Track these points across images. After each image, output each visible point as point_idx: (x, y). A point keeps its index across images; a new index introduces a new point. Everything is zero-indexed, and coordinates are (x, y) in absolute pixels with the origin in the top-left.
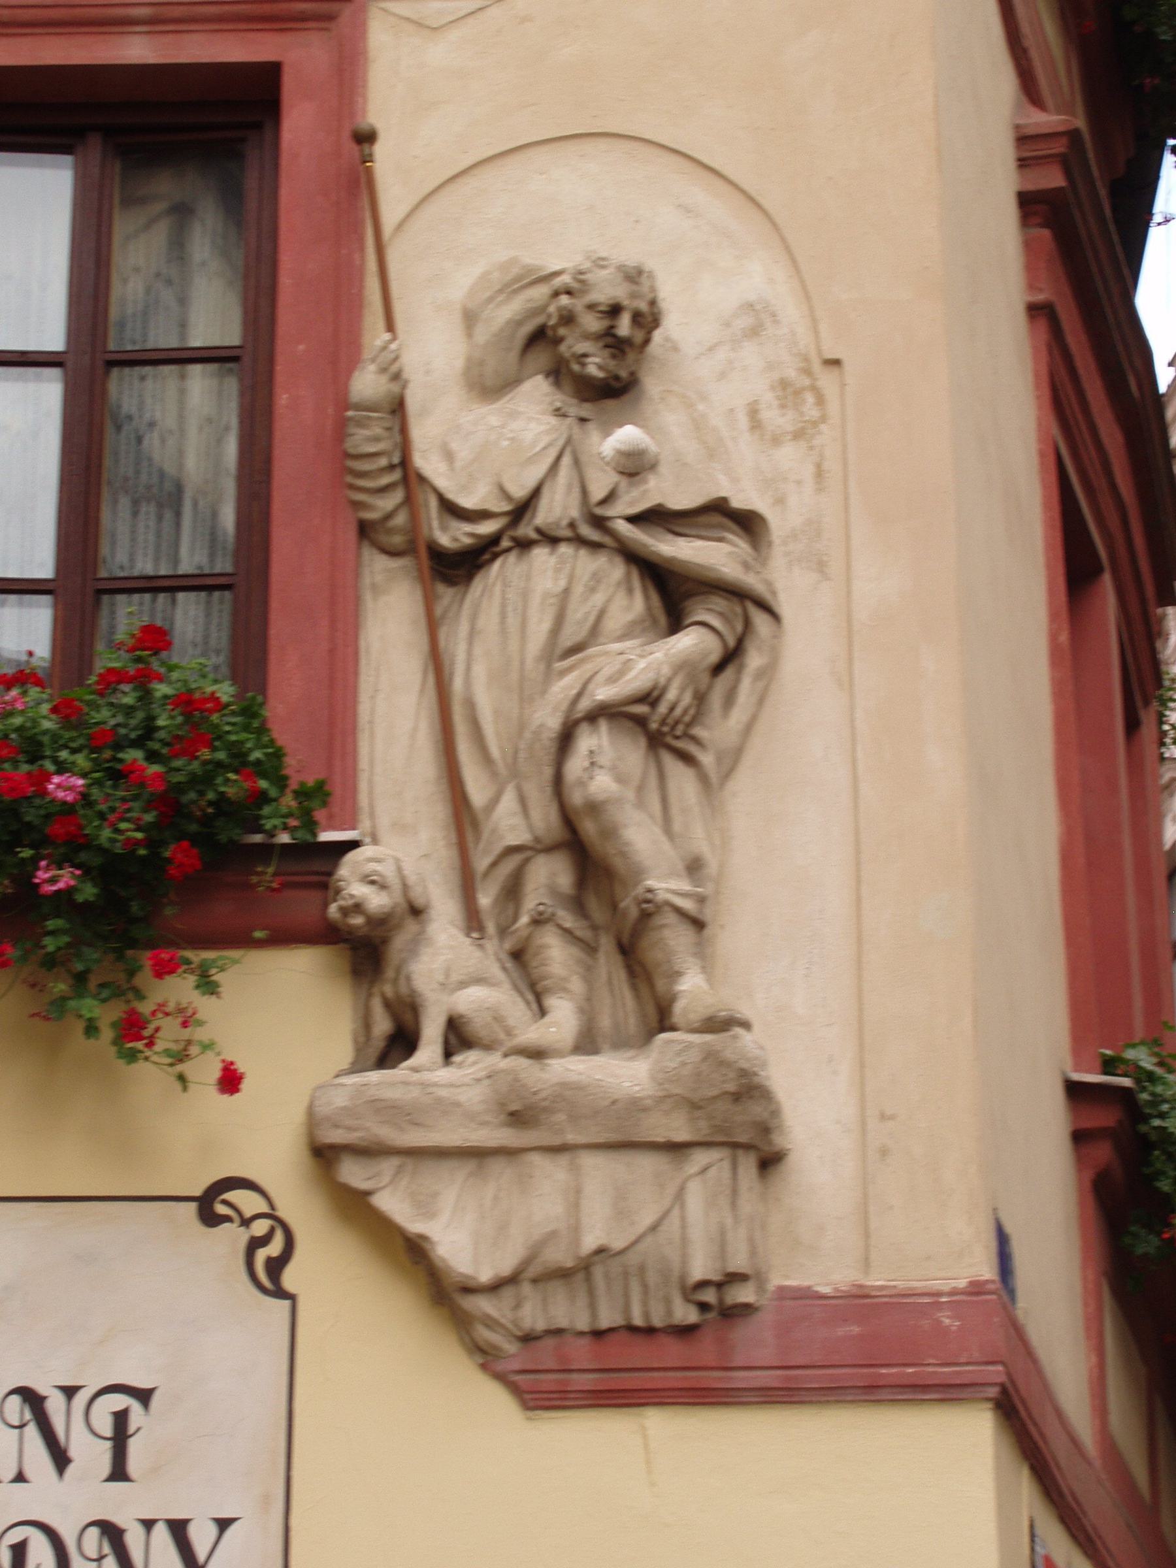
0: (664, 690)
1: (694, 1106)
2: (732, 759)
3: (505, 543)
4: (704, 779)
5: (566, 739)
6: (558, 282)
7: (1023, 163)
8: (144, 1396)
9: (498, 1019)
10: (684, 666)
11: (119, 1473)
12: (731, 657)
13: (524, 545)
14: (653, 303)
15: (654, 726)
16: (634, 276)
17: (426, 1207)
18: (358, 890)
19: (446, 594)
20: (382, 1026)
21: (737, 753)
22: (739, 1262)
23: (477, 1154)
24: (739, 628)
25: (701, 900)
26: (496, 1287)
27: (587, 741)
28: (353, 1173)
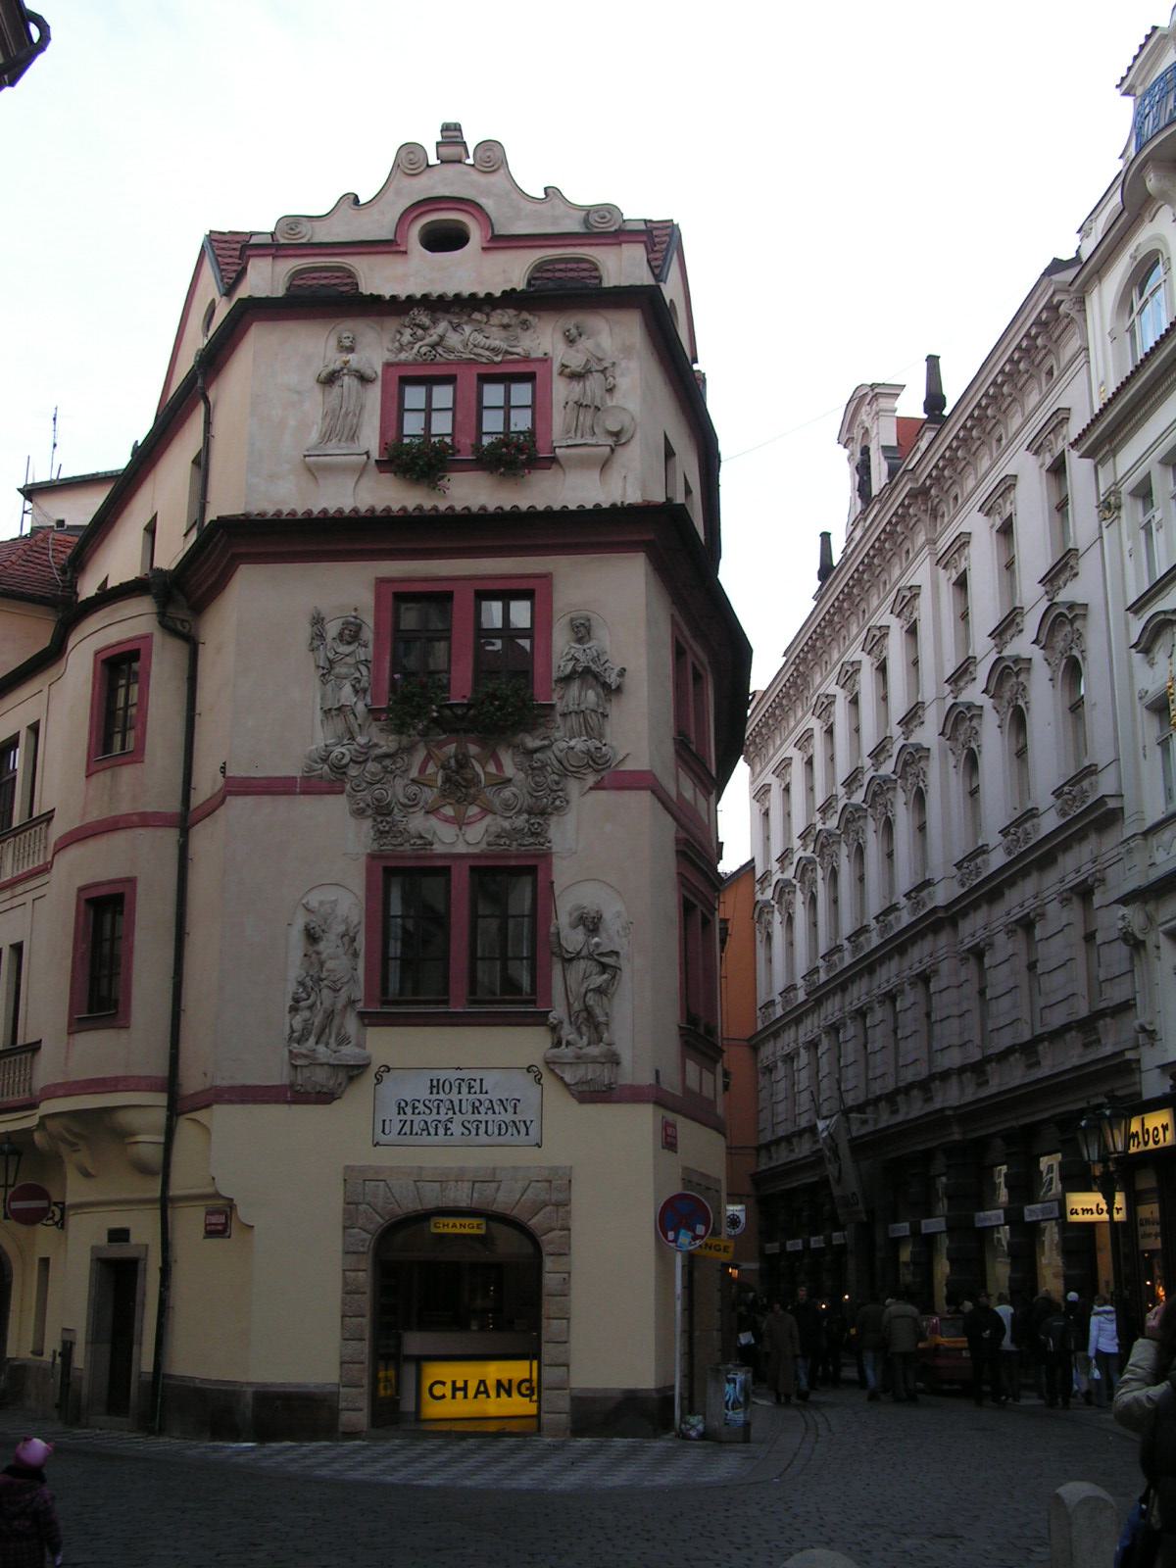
1: (605, 1057)
4: (609, 1000)
5: (586, 993)
6: (585, 911)
7: (677, 844)
8: (519, 1101)
10: (605, 981)
11: (515, 1113)
13: (579, 959)
14: (601, 917)
17: (563, 1072)
18: (552, 1020)
19: (566, 965)
20: (556, 1040)
21: (614, 994)
22: (612, 1080)
23: (571, 1063)
26: (574, 1085)
27: (590, 995)
28: (552, 1066)
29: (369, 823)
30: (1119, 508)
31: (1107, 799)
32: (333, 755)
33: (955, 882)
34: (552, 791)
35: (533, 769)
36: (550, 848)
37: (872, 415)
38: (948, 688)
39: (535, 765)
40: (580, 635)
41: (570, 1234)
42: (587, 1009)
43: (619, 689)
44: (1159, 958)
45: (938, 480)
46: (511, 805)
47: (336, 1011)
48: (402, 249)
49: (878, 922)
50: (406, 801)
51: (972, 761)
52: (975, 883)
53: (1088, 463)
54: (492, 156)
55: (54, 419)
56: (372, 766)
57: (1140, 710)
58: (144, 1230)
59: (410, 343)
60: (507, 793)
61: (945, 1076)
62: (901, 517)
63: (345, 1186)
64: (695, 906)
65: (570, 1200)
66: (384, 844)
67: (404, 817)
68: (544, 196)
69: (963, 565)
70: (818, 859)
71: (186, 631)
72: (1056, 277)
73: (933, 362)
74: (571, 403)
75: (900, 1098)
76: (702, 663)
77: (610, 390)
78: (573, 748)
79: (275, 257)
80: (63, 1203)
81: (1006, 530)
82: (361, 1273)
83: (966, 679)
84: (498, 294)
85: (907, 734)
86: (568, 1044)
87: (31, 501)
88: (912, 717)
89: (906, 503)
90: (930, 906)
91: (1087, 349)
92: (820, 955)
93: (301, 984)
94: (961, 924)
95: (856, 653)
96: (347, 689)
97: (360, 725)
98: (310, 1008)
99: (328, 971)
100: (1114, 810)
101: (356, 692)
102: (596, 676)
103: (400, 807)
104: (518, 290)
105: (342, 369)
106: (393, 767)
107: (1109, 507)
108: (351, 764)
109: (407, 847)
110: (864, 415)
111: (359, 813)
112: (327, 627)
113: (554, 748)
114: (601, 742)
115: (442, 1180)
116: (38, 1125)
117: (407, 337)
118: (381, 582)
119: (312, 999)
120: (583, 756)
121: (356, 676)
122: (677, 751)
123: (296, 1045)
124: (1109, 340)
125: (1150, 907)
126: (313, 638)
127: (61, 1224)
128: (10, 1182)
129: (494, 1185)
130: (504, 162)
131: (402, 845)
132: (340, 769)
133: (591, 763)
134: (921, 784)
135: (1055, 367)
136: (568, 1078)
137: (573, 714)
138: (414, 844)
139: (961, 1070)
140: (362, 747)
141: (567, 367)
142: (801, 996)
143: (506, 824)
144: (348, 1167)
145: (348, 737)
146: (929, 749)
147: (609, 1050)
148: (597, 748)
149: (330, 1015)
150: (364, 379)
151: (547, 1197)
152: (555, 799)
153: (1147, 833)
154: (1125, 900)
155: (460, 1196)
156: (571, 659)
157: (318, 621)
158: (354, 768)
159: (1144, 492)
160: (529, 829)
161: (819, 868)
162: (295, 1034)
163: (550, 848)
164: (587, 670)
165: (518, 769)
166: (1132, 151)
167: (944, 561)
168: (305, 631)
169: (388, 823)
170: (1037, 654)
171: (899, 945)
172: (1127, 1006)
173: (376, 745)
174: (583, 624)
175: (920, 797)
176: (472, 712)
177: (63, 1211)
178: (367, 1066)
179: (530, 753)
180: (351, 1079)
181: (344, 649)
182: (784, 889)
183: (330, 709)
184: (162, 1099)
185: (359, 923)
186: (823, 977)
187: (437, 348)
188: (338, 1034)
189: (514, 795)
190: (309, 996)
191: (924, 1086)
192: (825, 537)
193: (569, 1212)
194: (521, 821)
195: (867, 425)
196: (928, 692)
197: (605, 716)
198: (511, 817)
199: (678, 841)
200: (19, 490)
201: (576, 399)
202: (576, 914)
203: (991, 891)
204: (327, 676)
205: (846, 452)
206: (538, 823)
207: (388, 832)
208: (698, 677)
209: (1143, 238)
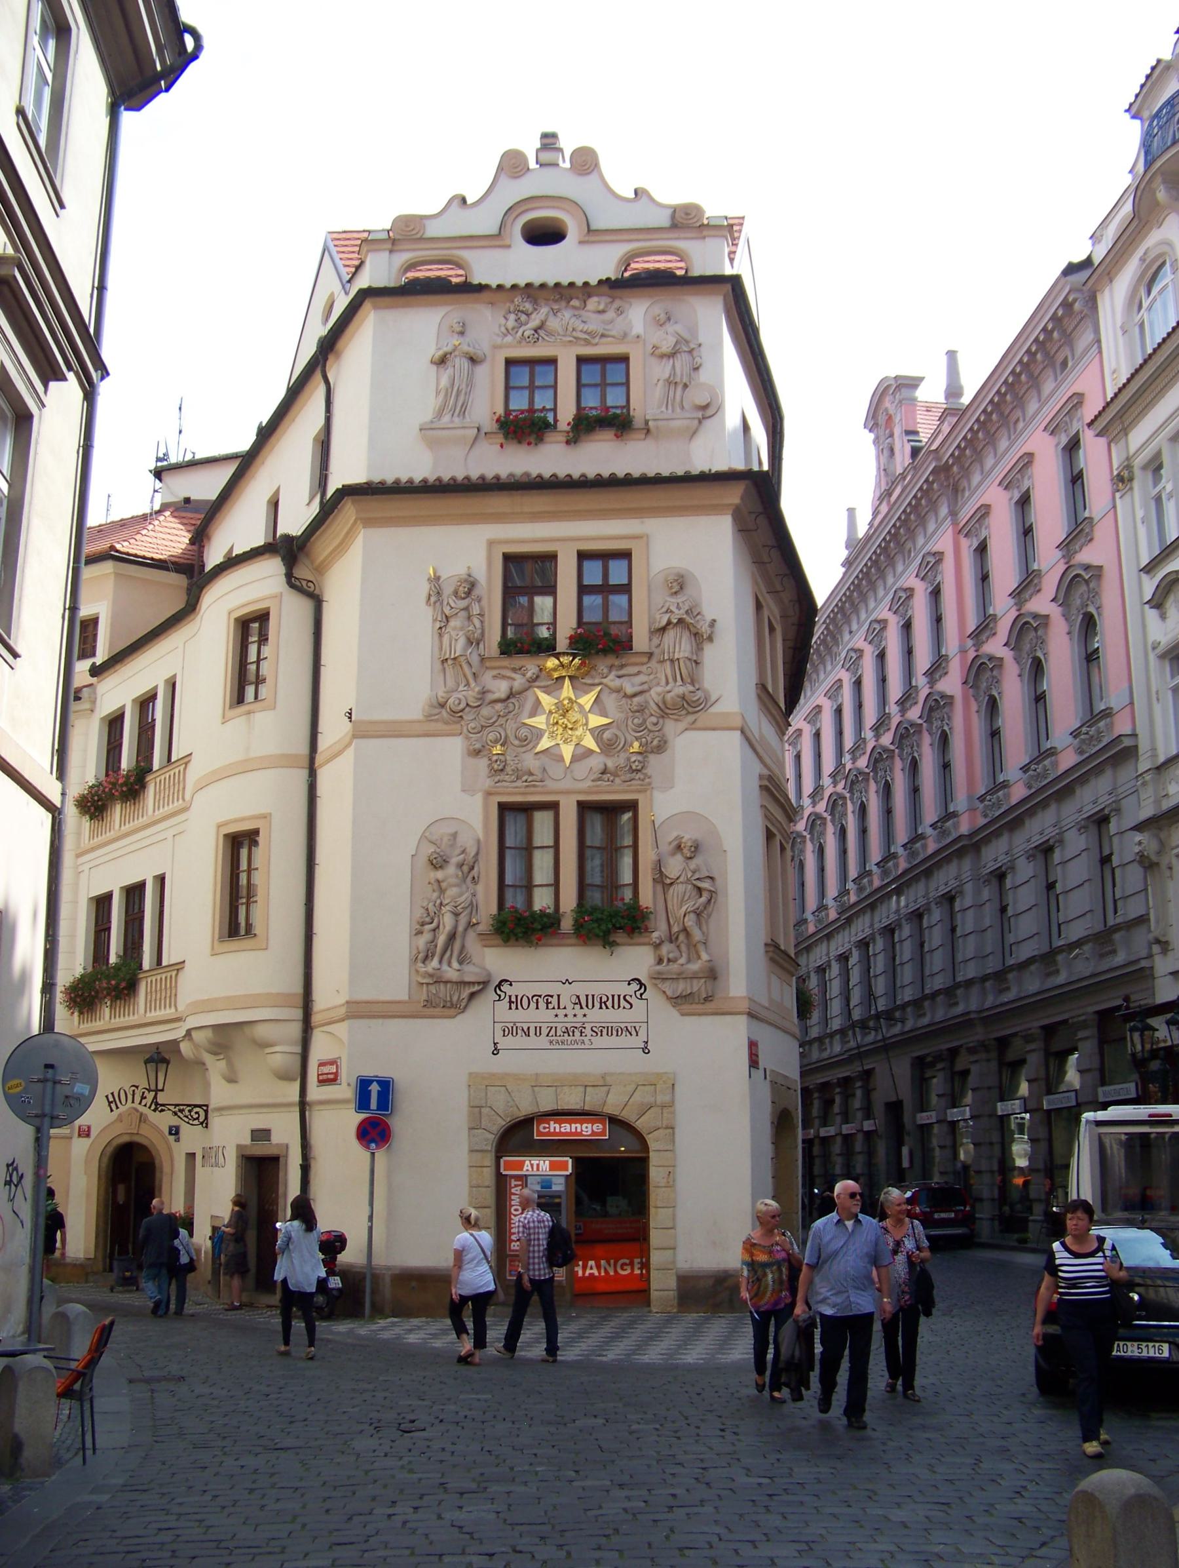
2: (709, 916)
12: (709, 901)
30: (1131, 479)
31: (1122, 738)
33: (978, 813)
34: (650, 731)
36: (650, 784)
37: (897, 402)
38: (970, 643)
40: (674, 590)
41: (674, 1133)
43: (710, 639)
44: (1171, 877)
45: (958, 459)
48: (507, 242)
49: (905, 850)
51: (993, 706)
52: (997, 814)
53: (1102, 441)
54: (586, 162)
55: (180, 409)
57: (1152, 657)
58: (285, 1132)
59: (513, 329)
61: (969, 983)
62: (926, 492)
63: (469, 1091)
65: (673, 1102)
66: (499, 781)
68: (633, 196)
69: (984, 533)
70: (848, 795)
71: (312, 589)
72: (1071, 278)
73: (952, 355)
74: (661, 382)
75: (927, 1004)
76: (774, 617)
77: (696, 369)
79: (391, 251)
80: (207, 1106)
81: (1024, 502)
82: (485, 1169)
83: (987, 634)
84: (594, 282)
85: (932, 683)
86: (669, 960)
87: (160, 480)
88: (938, 667)
89: (931, 479)
90: (954, 835)
91: (1099, 341)
92: (851, 879)
94: (984, 850)
95: (883, 612)
96: (462, 642)
98: (434, 930)
100: (1127, 749)
101: (470, 642)
104: (613, 278)
105: (454, 350)
107: (1122, 480)
108: (468, 709)
109: (519, 783)
110: (887, 403)
111: (477, 753)
112: (443, 586)
113: (652, 692)
114: (694, 686)
115: (558, 1083)
116: (184, 1037)
117: (511, 323)
118: (491, 544)
119: (436, 921)
123: (422, 965)
124: (1120, 333)
125: (1163, 835)
126: (430, 595)
127: (205, 1124)
128: (160, 1087)
129: (605, 1089)
130: (596, 165)
133: (685, 705)
134: (946, 728)
135: (1070, 358)
136: (669, 993)
138: (526, 781)
139: (984, 979)
141: (657, 348)
142: (833, 915)
144: (470, 1074)
146: (952, 697)
149: (452, 937)
150: (473, 360)
151: (653, 1099)
152: (654, 739)
153: (1160, 769)
154: (1139, 827)
155: (571, 1100)
156: (666, 612)
159: (1155, 467)
161: (849, 802)
164: (680, 621)
166: (1141, 168)
167: (964, 531)
168: (425, 588)
170: (1053, 611)
171: (925, 870)
172: (1142, 920)
173: (488, 691)
175: (944, 741)
177: (206, 1112)
178: (485, 984)
180: (472, 995)
181: (463, 604)
182: (815, 821)
184: (298, 1014)
185: (477, 854)
186: (853, 898)
187: (539, 331)
188: (461, 952)
189: (616, 735)
191: (949, 992)
192: (851, 512)
193: (673, 1113)
194: (621, 760)
195: (891, 412)
196: (952, 645)
199: (761, 777)
200: (151, 471)
201: (667, 376)
202: (676, 843)
203: (1014, 820)
205: (872, 436)
208: (772, 629)
209: (1153, 239)
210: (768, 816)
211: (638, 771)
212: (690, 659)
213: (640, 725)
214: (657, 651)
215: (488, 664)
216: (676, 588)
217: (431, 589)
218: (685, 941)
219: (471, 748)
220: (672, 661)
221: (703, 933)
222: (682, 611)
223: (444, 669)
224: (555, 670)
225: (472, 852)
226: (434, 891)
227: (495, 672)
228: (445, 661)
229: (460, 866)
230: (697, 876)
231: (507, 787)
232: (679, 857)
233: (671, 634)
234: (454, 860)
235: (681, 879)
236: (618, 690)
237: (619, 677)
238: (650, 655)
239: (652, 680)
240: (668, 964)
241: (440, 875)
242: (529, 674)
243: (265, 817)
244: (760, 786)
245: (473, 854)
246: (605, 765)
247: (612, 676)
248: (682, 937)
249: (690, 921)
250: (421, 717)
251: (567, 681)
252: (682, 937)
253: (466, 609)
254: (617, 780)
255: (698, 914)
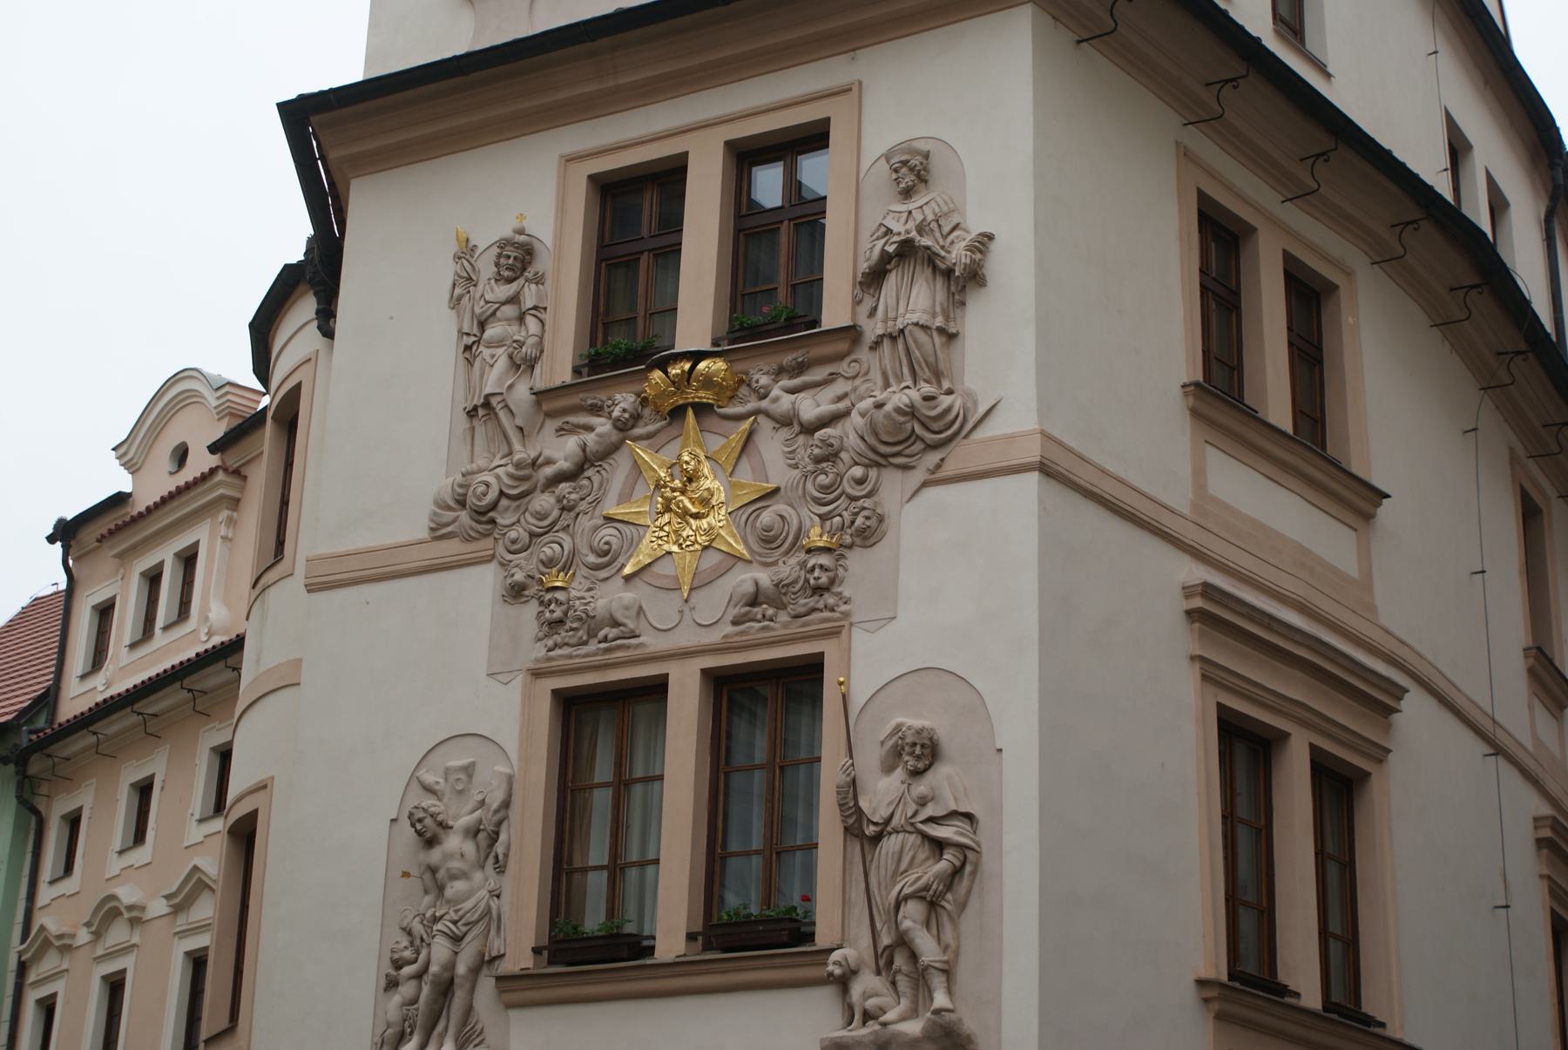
0: (931, 886)
2: (962, 906)
3: (885, 833)
9: (881, 1009)
10: (936, 877)
12: (957, 872)
13: (890, 834)
14: (931, 739)
15: (928, 899)
16: (919, 732)
18: (830, 968)
24: (962, 858)
25: (946, 962)
29: (533, 607)
32: (472, 489)
34: (854, 499)
35: (818, 460)
36: (846, 615)
39: (817, 451)
42: (903, 942)
43: (974, 277)
46: (775, 538)
47: (457, 981)
50: (592, 559)
56: (544, 501)
60: (767, 517)
64: (1285, 736)
66: (556, 646)
67: (590, 589)
78: (879, 406)
86: (867, 1016)
93: (409, 933)
96: (502, 363)
97: (521, 429)
98: (419, 976)
99: (448, 902)
101: (515, 365)
102: (931, 260)
103: (585, 571)
106: (573, 496)
108: (504, 502)
109: (592, 646)
111: (516, 592)
113: (854, 413)
120: (902, 419)
121: (516, 338)
122: (1194, 412)
131: (585, 643)
132: (485, 515)
133: (919, 430)
137: (886, 343)
138: (606, 637)
140: (518, 466)
143: (765, 577)
145: (498, 456)
147: (934, 1023)
148: (927, 398)
149: (445, 988)
157: (466, 252)
158: (507, 509)
160: (807, 581)
162: (390, 1031)
163: (846, 615)
164: (907, 251)
165: (790, 466)
168: (447, 271)
169: (560, 604)
173: (549, 462)
174: (904, 163)
176: (702, 365)
179: (809, 429)
181: (504, 291)
183: (475, 408)
185: (506, 804)
190: (418, 953)
194: (788, 568)
197: (951, 337)
198: (775, 563)
202: (891, 742)
204: (474, 348)
206: (821, 566)
207: (561, 622)
210: (1211, 674)
211: (819, 590)
212: (925, 328)
213: (825, 489)
214: (873, 329)
215: (545, 407)
216: (909, 179)
217: (456, 273)
218: (905, 968)
219: (509, 581)
220: (893, 338)
221: (946, 949)
222: (911, 225)
223: (473, 429)
224: (663, 395)
225: (495, 800)
226: (426, 892)
227: (558, 423)
228: (472, 413)
229: (473, 832)
230: (929, 811)
231: (570, 657)
232: (899, 774)
233: (892, 281)
234: (466, 820)
235: (895, 822)
236: (785, 421)
237: (792, 391)
238: (851, 333)
239: (855, 389)
240: (864, 1023)
241: (435, 855)
242: (616, 413)
243: (265, 787)
244: (1189, 613)
245: (495, 806)
246: (757, 584)
247: (776, 392)
248: (900, 961)
249: (911, 916)
250: (424, 534)
251: (690, 412)
252: (900, 961)
253: (514, 300)
254: (783, 617)
255: (932, 902)
